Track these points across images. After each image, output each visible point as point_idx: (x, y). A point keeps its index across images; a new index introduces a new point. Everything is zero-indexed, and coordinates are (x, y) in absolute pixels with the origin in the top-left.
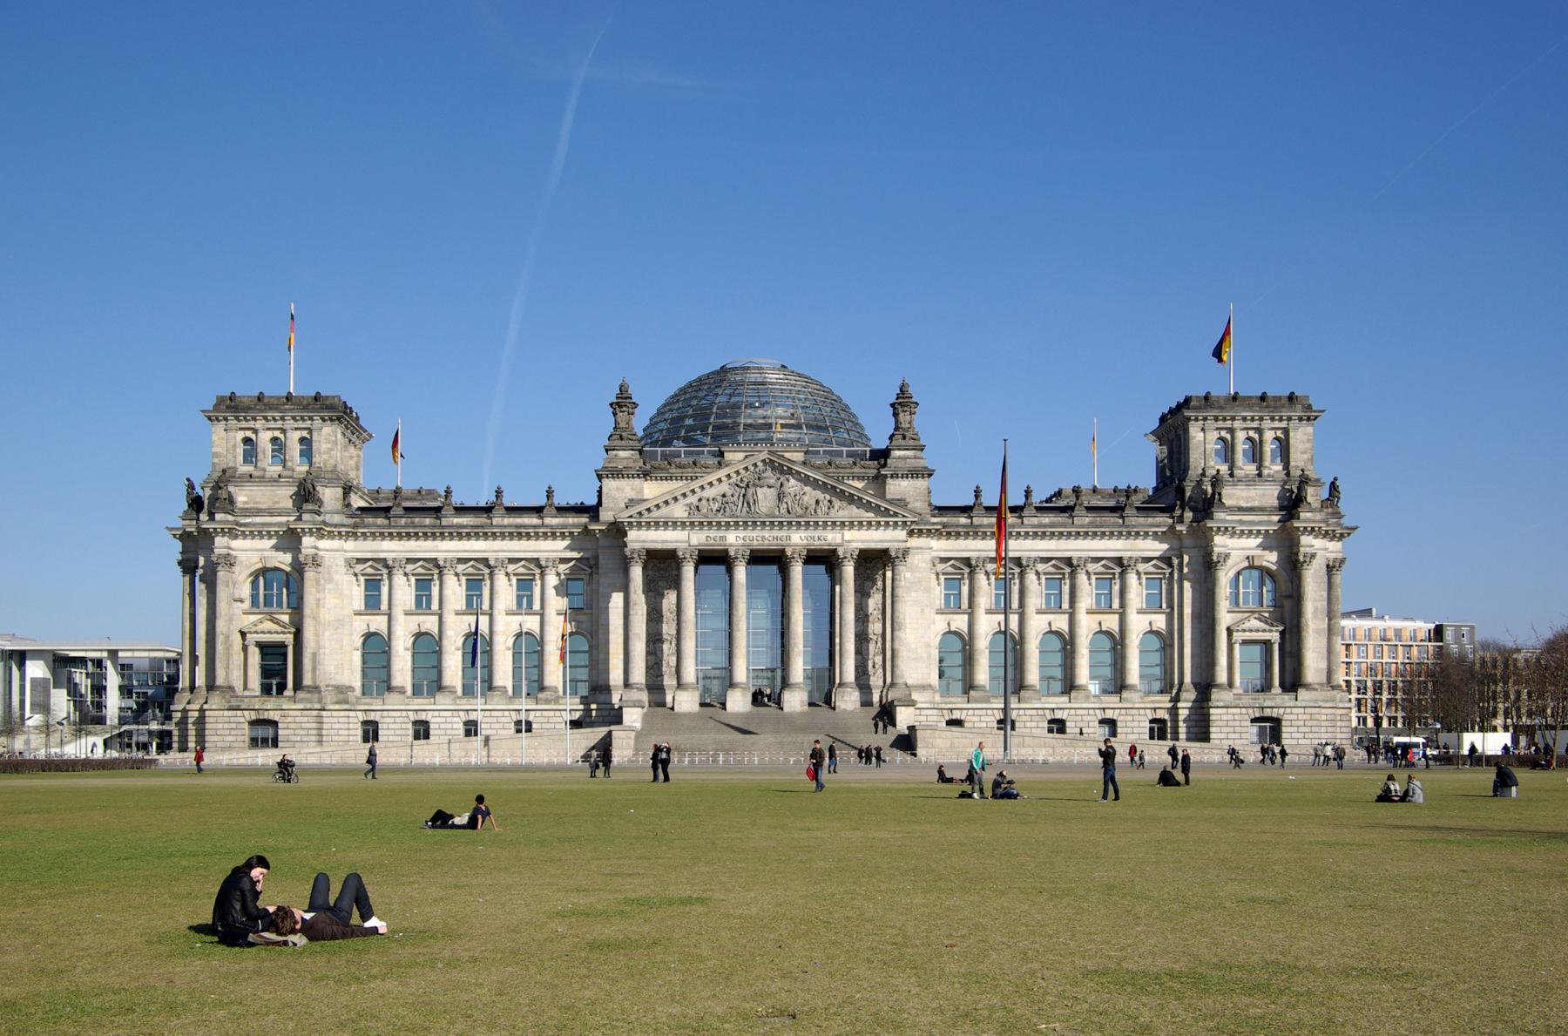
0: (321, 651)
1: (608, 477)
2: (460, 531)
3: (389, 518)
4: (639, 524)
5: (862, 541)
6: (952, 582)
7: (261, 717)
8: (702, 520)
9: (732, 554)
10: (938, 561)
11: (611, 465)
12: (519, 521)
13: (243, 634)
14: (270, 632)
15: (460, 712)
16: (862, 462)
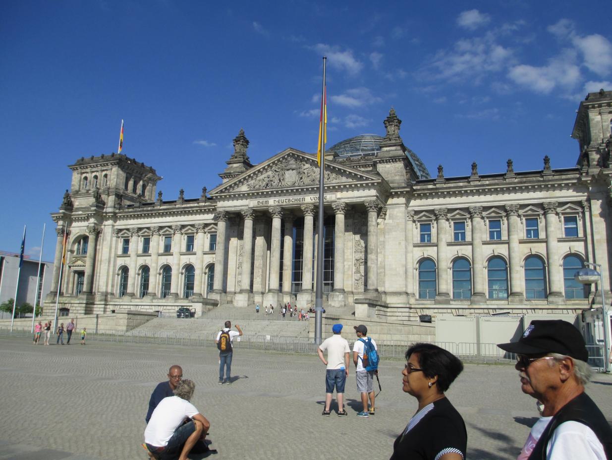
0: (98, 274)
1: (225, 178)
2: (159, 212)
3: (133, 208)
4: (221, 196)
5: (348, 198)
6: (425, 228)
7: (63, 307)
8: (253, 192)
9: (271, 211)
10: (414, 213)
11: (228, 172)
12: (188, 205)
13: (70, 267)
14: (78, 266)
15: (153, 307)
16: (366, 157)
